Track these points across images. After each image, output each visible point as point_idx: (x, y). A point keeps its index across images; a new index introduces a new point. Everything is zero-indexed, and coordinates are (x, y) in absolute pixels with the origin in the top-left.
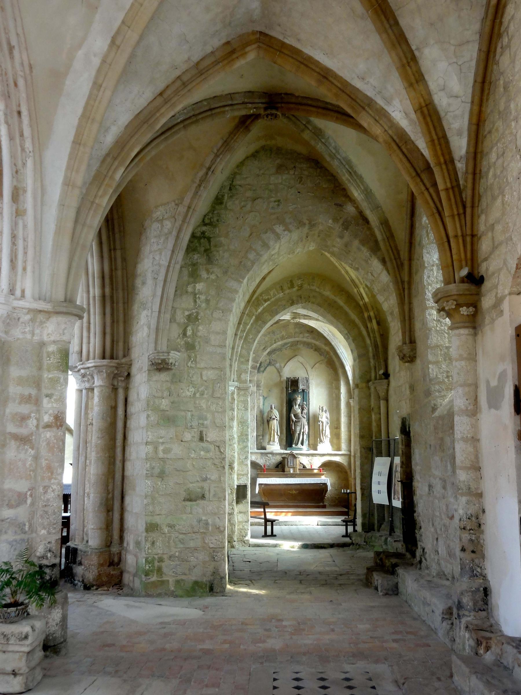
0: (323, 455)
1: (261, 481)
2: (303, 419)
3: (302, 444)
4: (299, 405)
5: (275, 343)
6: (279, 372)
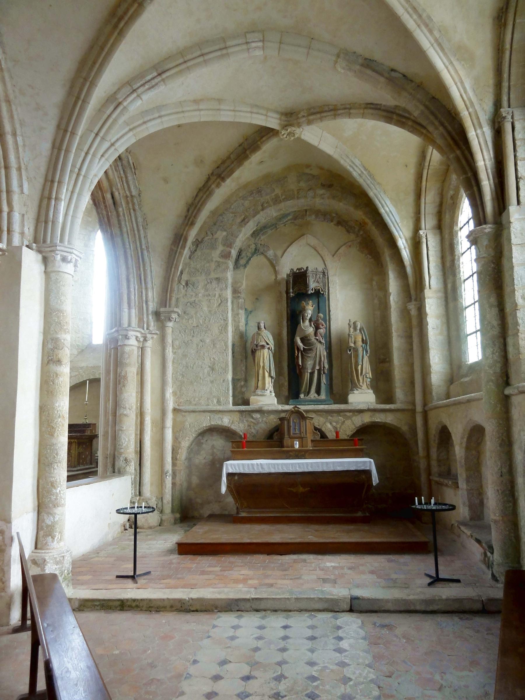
0: (361, 411)
1: (233, 466)
2: (319, 345)
3: (318, 392)
5: (263, 210)
6: (273, 265)
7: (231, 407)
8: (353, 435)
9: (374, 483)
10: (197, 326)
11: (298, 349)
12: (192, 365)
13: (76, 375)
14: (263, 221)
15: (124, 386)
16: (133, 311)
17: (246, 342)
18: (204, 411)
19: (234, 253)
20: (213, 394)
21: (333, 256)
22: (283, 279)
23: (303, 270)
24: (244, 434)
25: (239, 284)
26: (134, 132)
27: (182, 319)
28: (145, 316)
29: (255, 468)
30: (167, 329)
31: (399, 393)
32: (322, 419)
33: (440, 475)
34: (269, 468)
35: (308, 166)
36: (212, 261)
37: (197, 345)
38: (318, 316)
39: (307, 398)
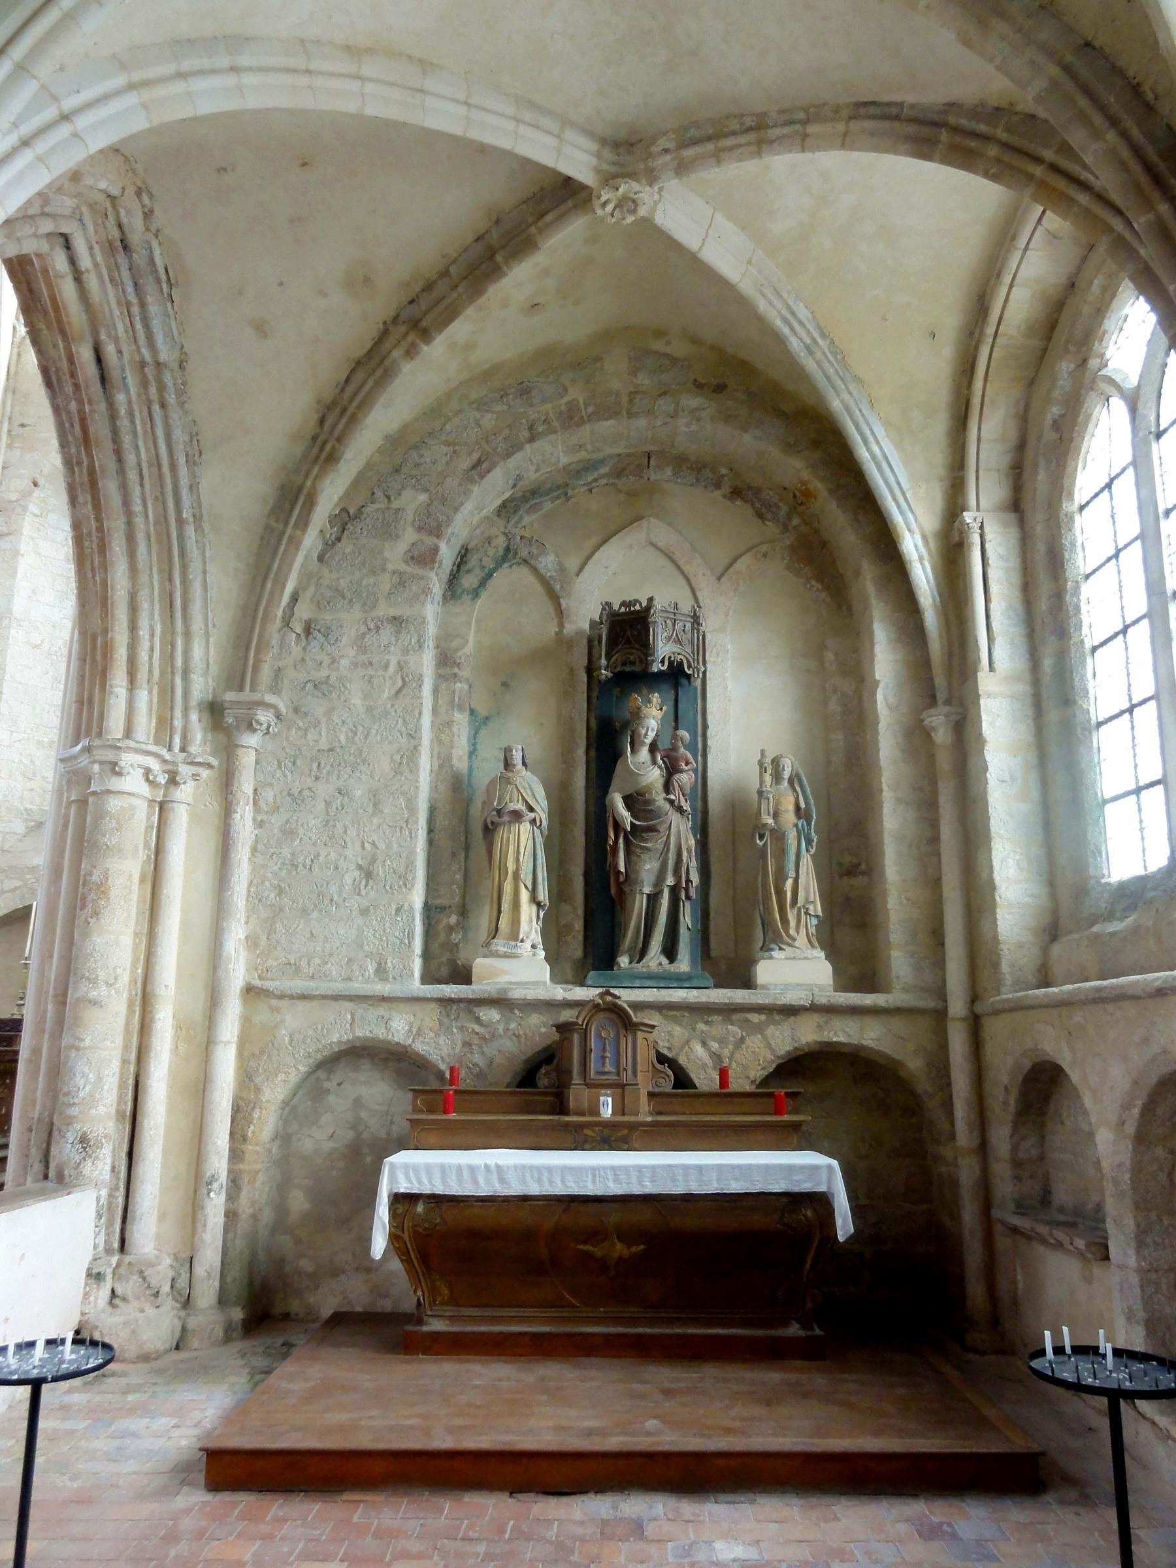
0: (791, 1011)
2: (675, 818)
3: (670, 951)
4: (653, 748)
5: (532, 439)
7: (415, 986)
8: (766, 1081)
9: (839, 1233)
10: (331, 750)
11: (617, 826)
12: (308, 862)
13: (16, 888)
14: (532, 476)
15: (96, 913)
16: (143, 698)
17: (468, 802)
18: (336, 998)
19: (447, 554)
20: (366, 948)
21: (719, 579)
22: (580, 633)
23: (638, 607)
24: (452, 1069)
25: (454, 644)
26: (147, 94)
27: (289, 729)
28: (178, 713)
29: (481, 1180)
30: (240, 752)
31: (900, 962)
32: (678, 1030)
33: (1021, 1208)
34: (523, 1181)
35: (660, 334)
36: (384, 570)
37: (327, 804)
38: (675, 737)
39: (639, 968)
